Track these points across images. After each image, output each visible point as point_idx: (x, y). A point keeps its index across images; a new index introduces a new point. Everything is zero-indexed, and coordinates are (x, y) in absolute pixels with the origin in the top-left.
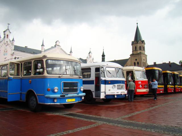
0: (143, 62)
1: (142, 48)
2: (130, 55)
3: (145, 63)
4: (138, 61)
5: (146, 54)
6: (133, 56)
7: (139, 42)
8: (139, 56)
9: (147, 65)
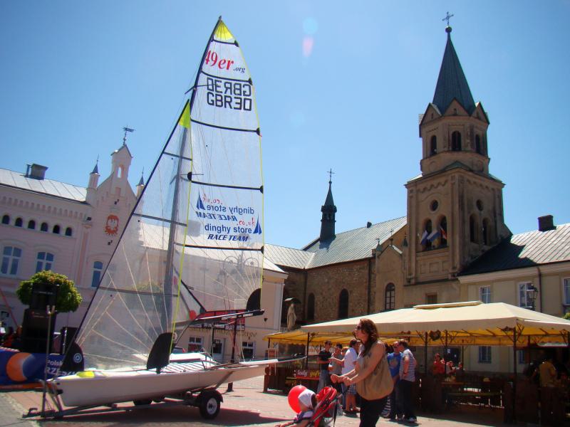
1: (465, 141)
2: (413, 188)
3: (485, 222)
4: (443, 210)
5: (494, 170)
7: (451, 110)
8: (446, 181)
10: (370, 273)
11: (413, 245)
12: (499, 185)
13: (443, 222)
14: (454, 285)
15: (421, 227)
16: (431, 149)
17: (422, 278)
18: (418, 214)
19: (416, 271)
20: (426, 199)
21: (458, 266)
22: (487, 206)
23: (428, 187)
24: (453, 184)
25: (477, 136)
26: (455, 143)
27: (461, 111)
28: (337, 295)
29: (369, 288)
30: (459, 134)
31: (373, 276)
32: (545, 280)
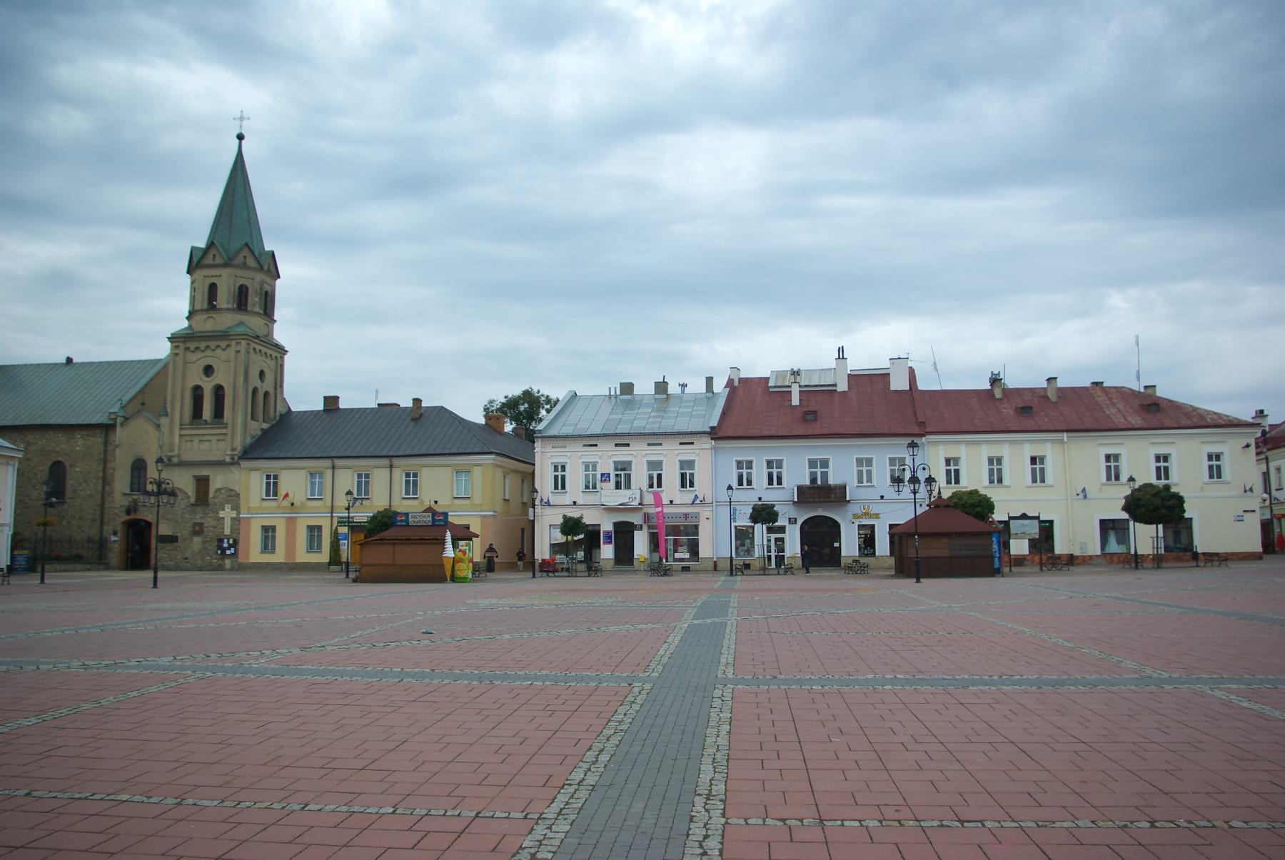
0: (255, 391)
1: (254, 301)
2: (172, 339)
3: (266, 394)
4: (220, 378)
5: (280, 334)
6: (192, 346)
8: (229, 346)
9: (284, 411)
10: (106, 443)
11: (177, 416)
12: (282, 351)
13: (219, 392)
14: (233, 468)
16: (206, 302)
17: (186, 457)
18: (184, 376)
19: (180, 448)
21: (239, 448)
22: (269, 376)
27: (251, 262)
28: (45, 468)
29: (105, 461)
31: (110, 448)
32: (339, 473)
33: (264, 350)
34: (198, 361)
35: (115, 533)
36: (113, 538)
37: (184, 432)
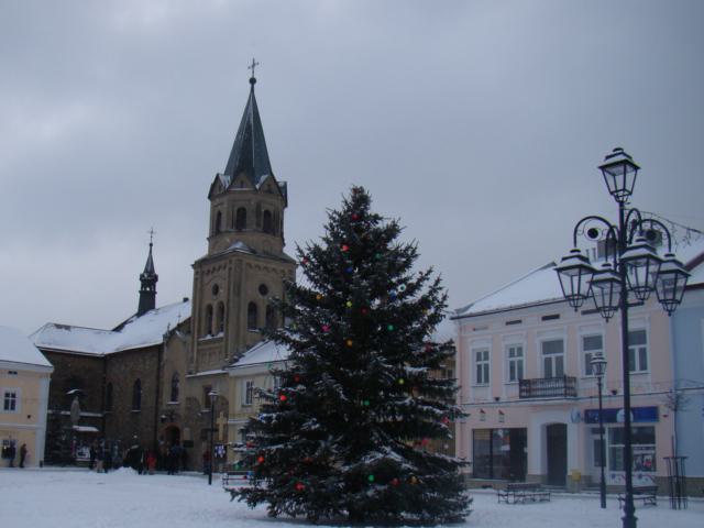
6: (205, 268)
10: (160, 360)
13: (221, 308)
15: (204, 314)
20: (210, 282)
23: (211, 269)
24: (230, 269)
25: (267, 213)
26: (240, 221)
29: (158, 377)
30: (244, 209)
33: (262, 264)
34: (210, 282)
35: (162, 438)
36: (162, 443)
37: (200, 347)
